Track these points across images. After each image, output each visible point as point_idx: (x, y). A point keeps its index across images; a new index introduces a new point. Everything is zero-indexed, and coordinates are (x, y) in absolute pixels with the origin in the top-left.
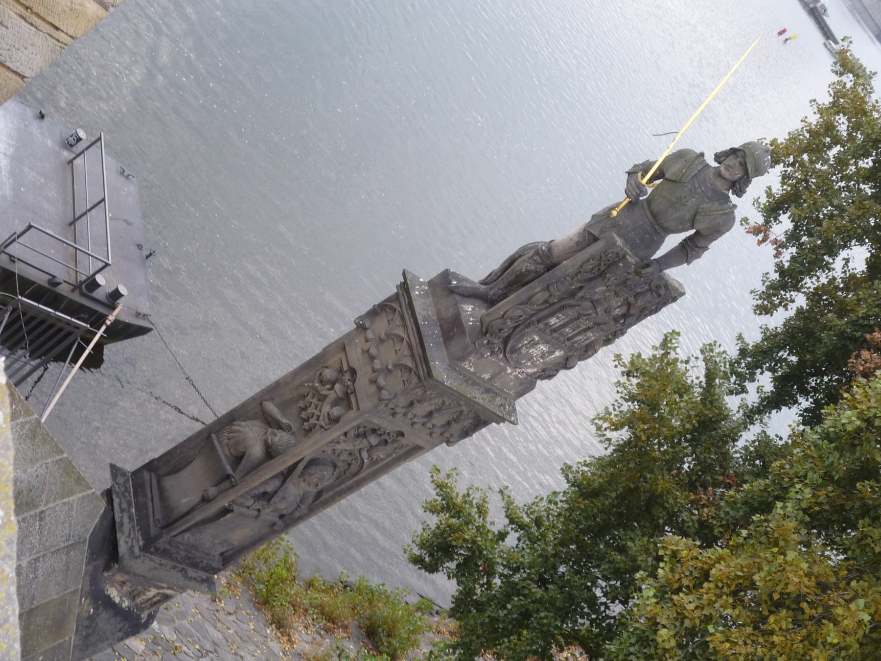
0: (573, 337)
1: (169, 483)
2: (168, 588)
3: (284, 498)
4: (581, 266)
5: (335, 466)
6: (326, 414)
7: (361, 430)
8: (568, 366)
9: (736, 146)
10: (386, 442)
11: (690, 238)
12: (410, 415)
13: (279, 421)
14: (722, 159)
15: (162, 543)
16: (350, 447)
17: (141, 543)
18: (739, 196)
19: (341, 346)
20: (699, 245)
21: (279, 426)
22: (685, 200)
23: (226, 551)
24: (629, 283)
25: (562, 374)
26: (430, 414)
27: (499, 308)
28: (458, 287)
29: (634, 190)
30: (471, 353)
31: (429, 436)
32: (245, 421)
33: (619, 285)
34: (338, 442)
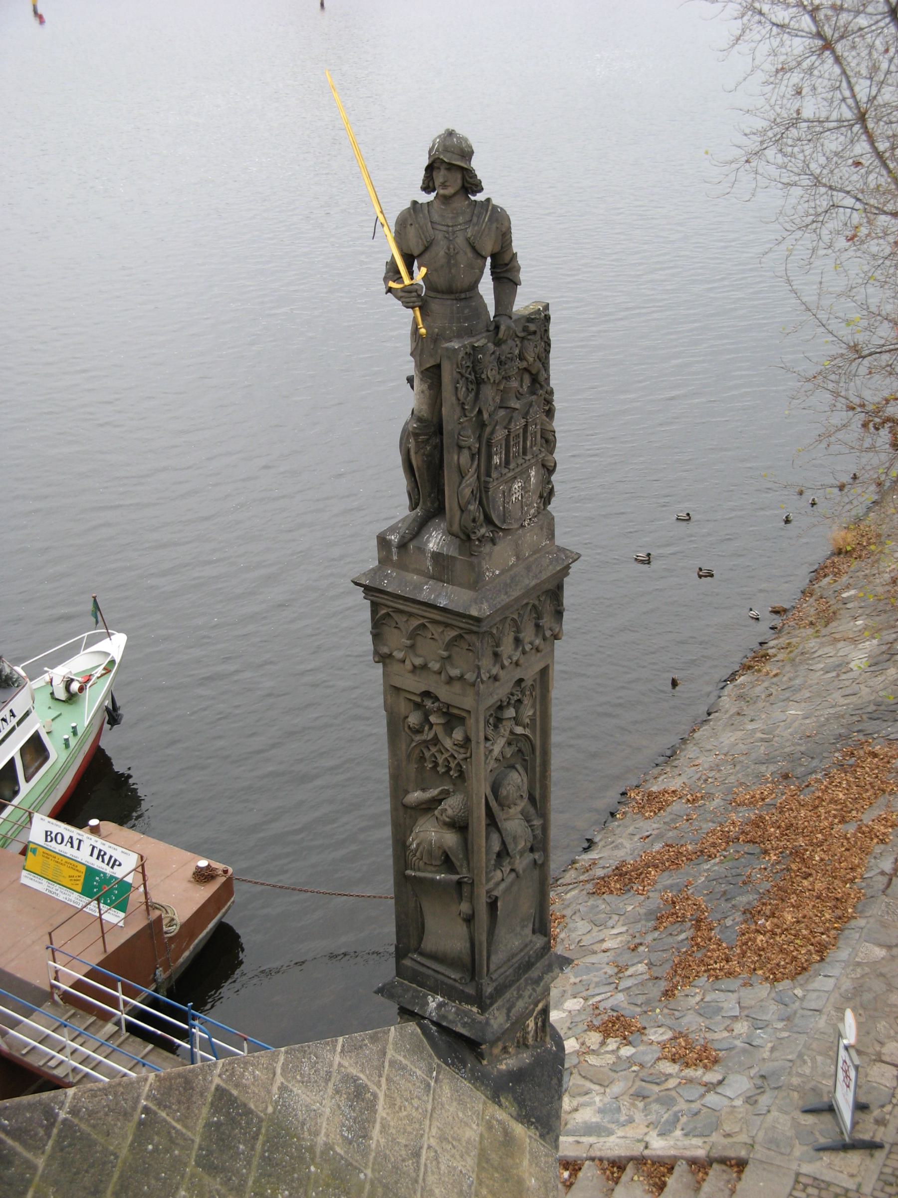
0: (525, 448)
1: (429, 944)
2: (536, 1005)
3: (515, 838)
4: (459, 400)
5: (513, 767)
6: (455, 747)
7: (491, 721)
8: (551, 469)
9: (425, 162)
10: (519, 701)
11: (493, 266)
12: (506, 663)
13: (433, 797)
14: (431, 185)
15: (489, 990)
16: (501, 742)
17: (475, 1009)
19: (393, 690)
20: (506, 262)
21: (437, 801)
22: (452, 250)
23: (534, 925)
24: (503, 358)
25: (553, 478)
26: (518, 641)
27: (451, 510)
28: (403, 537)
29: (409, 298)
30: (480, 563)
31: (539, 654)
32: (412, 832)
33: (499, 369)
34: (491, 751)
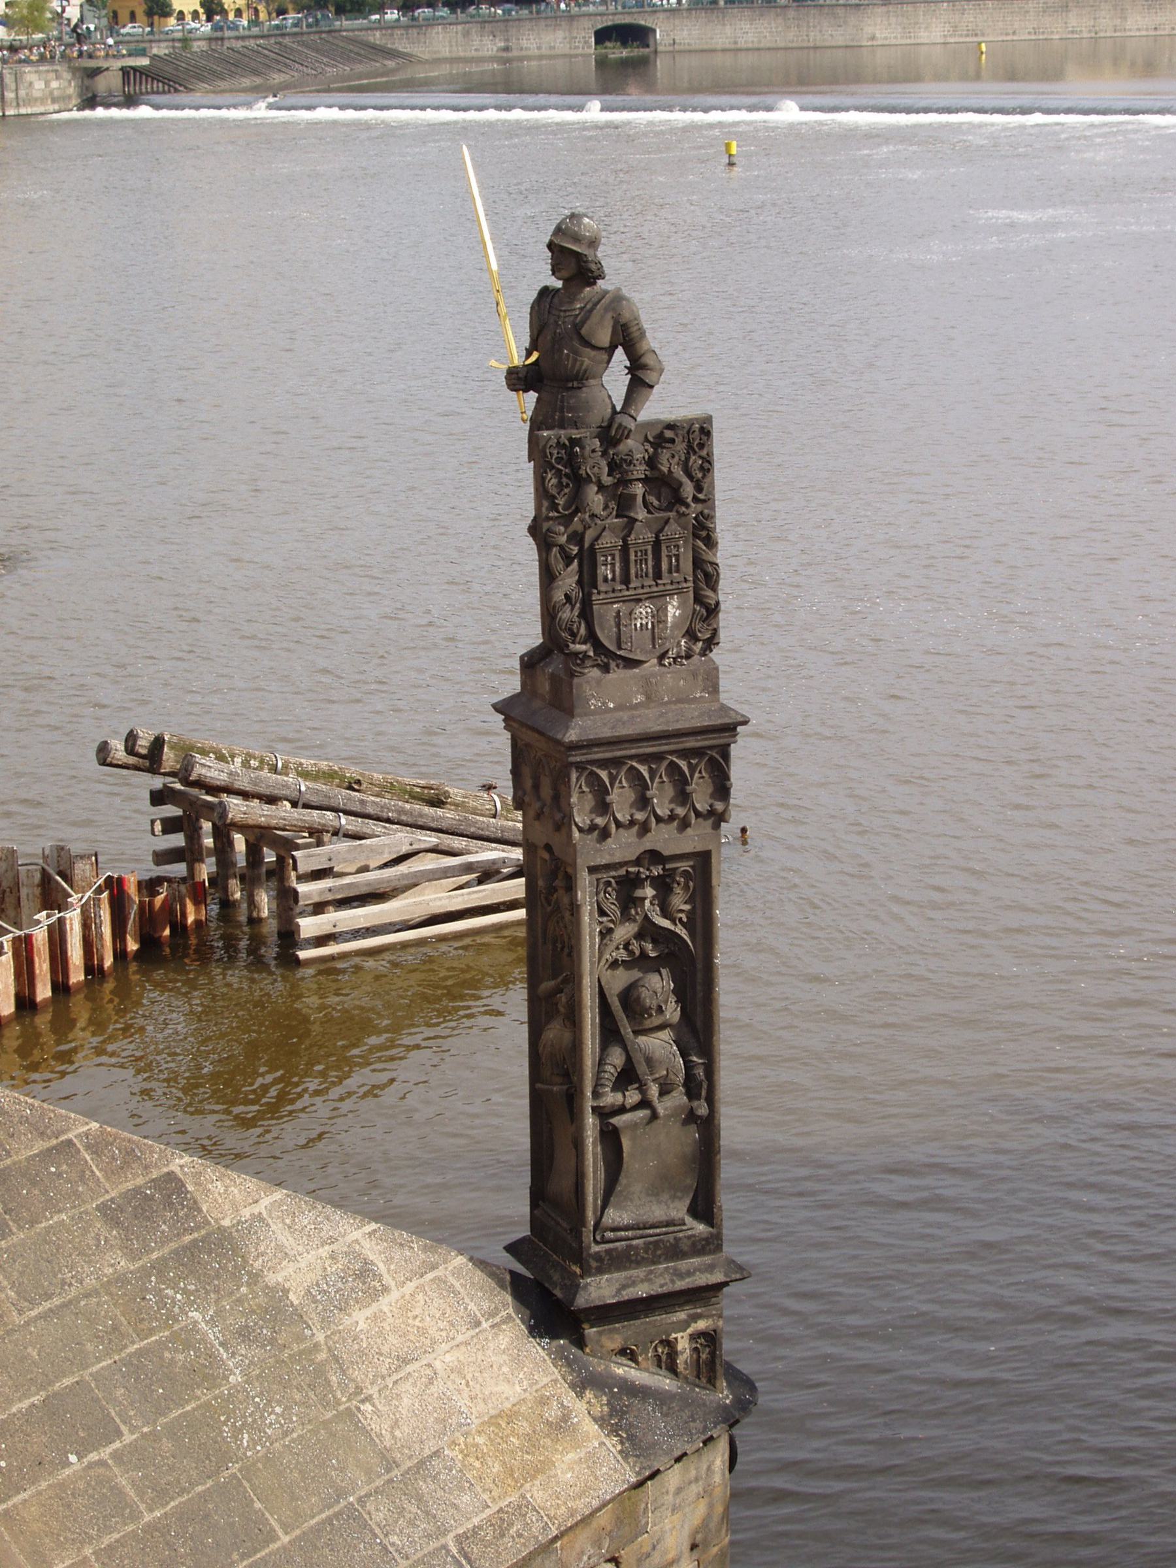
18: (601, 276)
